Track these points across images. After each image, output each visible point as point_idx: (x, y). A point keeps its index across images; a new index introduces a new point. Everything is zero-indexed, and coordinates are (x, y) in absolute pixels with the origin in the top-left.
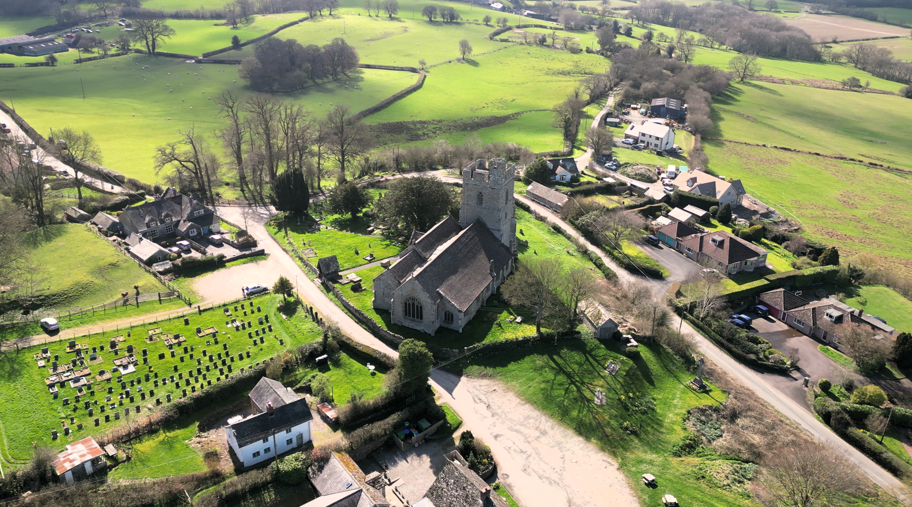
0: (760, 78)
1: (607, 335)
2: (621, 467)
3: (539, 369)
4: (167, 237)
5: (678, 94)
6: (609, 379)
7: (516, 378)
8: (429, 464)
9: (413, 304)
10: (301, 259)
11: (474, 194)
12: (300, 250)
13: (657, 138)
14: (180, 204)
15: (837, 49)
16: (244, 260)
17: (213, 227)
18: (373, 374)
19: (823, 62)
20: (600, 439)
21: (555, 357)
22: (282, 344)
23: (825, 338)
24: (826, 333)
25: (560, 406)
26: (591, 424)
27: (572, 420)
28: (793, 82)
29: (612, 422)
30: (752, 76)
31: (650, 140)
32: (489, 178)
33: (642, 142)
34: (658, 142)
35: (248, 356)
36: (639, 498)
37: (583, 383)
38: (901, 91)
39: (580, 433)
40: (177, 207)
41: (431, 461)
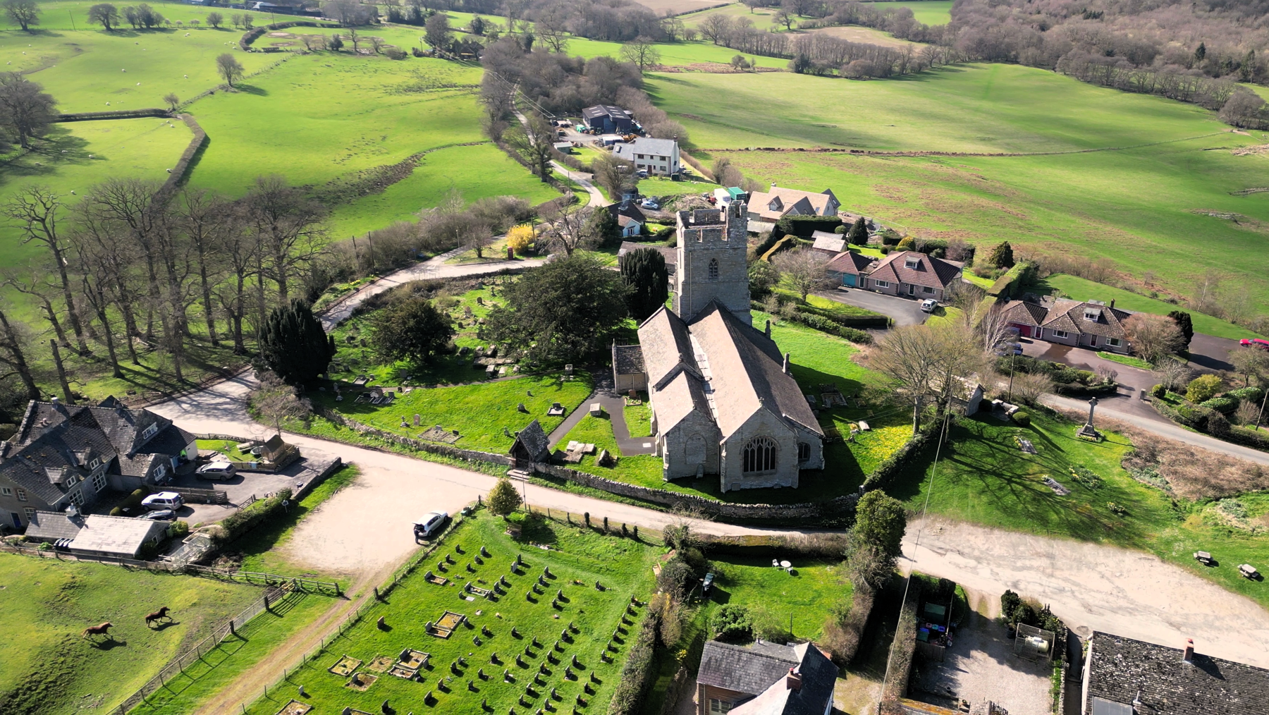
0: (660, 68)
1: (975, 408)
2: (1163, 557)
3: (956, 480)
4: (117, 498)
5: (609, 96)
6: (1038, 459)
7: (945, 502)
8: (993, 662)
9: (760, 449)
10: (432, 450)
11: (705, 264)
13: (663, 158)
14: (95, 425)
15: (689, 23)
16: (324, 488)
17: (188, 453)
18: (794, 573)
19: (679, 42)
20: (1108, 536)
21: (956, 457)
22: (602, 589)
23: (1093, 343)
24: (1095, 336)
25: (1030, 516)
26: (1082, 521)
27: (1059, 525)
28: (688, 70)
29: (1100, 510)
30: (652, 66)
31: (652, 163)
32: (729, 233)
33: (641, 166)
34: (665, 164)
35: (576, 631)
36: (1219, 583)
37: (1020, 477)
38: (789, 66)
39: (1085, 539)
40: (92, 433)
41: (991, 655)
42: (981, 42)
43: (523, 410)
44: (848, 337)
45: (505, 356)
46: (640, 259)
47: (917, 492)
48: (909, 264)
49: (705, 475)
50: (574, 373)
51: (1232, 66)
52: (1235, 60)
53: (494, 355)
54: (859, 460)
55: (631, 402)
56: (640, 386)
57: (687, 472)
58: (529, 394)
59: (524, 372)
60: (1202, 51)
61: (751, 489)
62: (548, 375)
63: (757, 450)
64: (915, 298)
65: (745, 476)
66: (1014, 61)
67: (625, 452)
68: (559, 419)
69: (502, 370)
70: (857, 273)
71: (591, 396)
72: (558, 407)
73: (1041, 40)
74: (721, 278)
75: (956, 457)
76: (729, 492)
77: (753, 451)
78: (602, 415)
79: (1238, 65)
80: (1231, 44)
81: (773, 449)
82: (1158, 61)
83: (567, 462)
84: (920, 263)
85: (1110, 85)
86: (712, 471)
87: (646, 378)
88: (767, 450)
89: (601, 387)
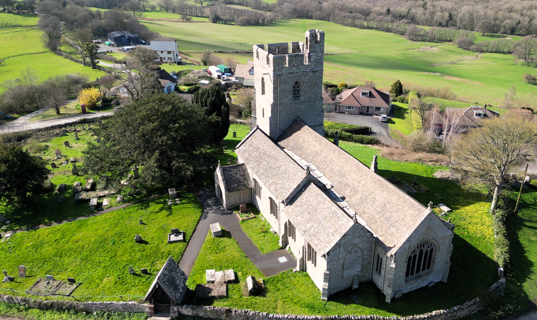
11: (289, 87)
12: (21, 293)
21: (527, 224)
32: (309, 57)
42: (295, 10)
43: (140, 241)
44: (362, 142)
45: (105, 188)
46: (209, 97)
47: (531, 264)
48: (364, 94)
49: (361, 284)
50: (178, 196)
51: (401, 17)
52: (403, 14)
53: (93, 188)
54: (467, 240)
55: (245, 216)
56: (247, 200)
57: (343, 285)
58: (142, 223)
59: (129, 201)
60: (388, 11)
61: (410, 293)
62: (153, 201)
63: (418, 255)
64: (371, 115)
65: (407, 281)
66: (311, 18)
67: (265, 272)
68: (181, 245)
69: (105, 202)
70: (333, 102)
71: (203, 216)
72: (176, 232)
73: (321, 8)
74: (302, 98)
75: (527, 224)
76: (393, 300)
77: (415, 256)
78: (224, 234)
79: (404, 17)
80: (400, 7)
81: (432, 250)
82: (372, 15)
83: (214, 298)
84: (370, 93)
85: (355, 26)
86: (364, 280)
87: (254, 192)
88: (427, 251)
89: (209, 206)
